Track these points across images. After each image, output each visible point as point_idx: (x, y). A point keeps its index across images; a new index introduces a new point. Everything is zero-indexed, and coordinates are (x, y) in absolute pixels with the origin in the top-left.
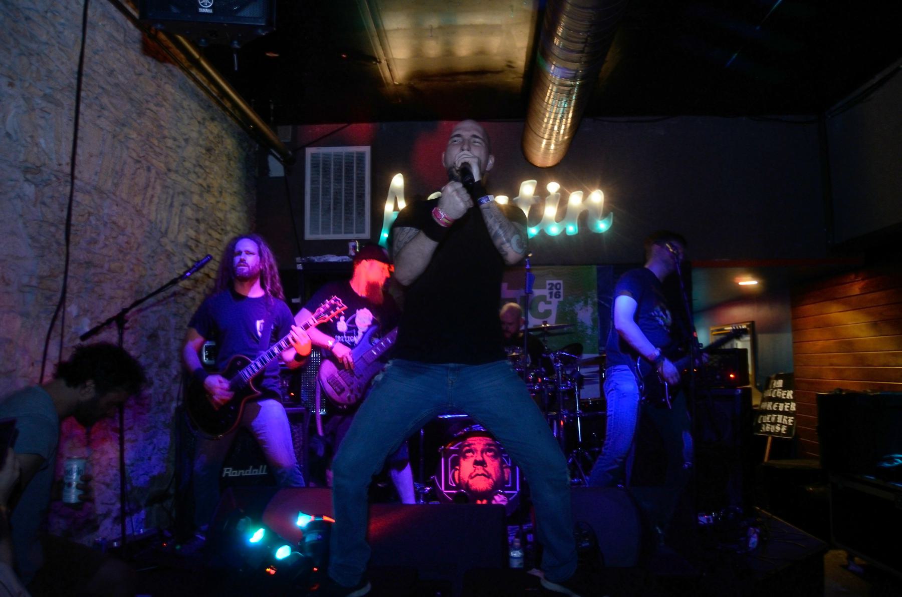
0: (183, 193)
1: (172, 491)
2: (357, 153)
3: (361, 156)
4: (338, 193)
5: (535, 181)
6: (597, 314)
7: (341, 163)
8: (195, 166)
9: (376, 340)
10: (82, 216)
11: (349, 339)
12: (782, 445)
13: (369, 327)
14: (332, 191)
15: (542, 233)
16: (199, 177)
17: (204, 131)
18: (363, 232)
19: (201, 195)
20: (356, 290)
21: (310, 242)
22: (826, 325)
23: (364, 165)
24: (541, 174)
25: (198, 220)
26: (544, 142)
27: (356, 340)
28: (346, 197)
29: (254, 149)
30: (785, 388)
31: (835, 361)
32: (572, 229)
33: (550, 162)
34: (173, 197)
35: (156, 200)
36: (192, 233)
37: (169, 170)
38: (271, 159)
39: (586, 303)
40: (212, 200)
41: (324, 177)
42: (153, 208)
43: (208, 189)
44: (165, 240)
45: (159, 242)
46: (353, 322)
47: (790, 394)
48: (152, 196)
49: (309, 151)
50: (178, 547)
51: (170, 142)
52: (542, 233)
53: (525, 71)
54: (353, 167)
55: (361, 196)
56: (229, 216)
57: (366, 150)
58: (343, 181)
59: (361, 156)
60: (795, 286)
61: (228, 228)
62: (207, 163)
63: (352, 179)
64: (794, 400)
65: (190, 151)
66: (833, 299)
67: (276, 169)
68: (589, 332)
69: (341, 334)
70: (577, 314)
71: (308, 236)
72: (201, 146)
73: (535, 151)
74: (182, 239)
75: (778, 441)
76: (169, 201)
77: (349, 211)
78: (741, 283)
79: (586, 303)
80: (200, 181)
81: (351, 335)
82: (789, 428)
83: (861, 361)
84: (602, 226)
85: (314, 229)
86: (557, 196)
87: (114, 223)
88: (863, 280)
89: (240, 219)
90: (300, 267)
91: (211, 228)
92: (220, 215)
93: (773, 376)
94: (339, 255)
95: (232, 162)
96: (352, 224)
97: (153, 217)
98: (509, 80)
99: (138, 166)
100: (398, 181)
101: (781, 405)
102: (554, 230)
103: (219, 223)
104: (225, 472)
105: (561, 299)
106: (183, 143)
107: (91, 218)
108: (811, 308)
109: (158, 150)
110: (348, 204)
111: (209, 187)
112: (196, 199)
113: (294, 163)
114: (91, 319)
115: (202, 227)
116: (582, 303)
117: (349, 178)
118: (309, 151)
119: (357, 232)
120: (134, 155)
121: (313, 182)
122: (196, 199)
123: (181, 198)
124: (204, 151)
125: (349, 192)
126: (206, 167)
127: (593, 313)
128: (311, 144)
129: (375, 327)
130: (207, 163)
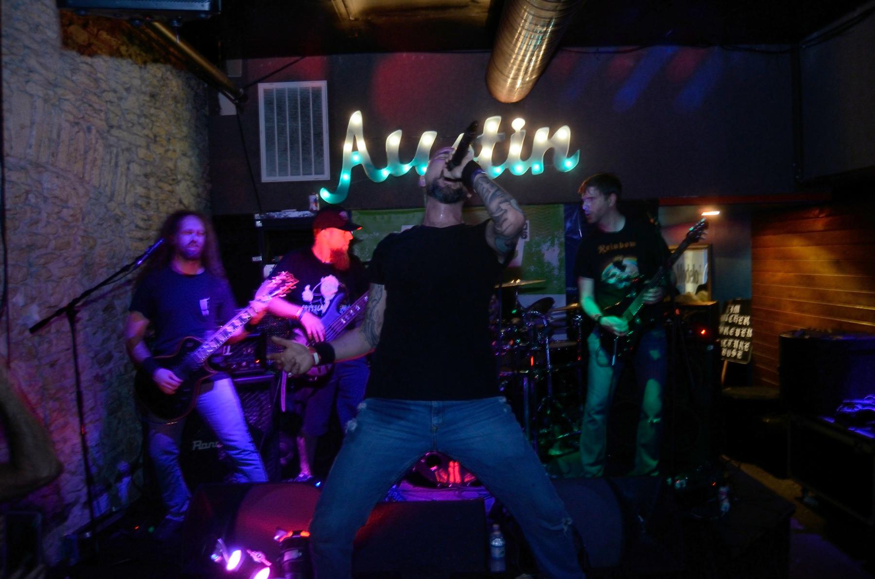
0: (128, 150)
1: (141, 461)
2: (313, 88)
3: (317, 93)
4: (294, 132)
5: (499, 118)
6: (564, 254)
7: (296, 100)
8: (139, 116)
9: (344, 308)
10: (20, 196)
11: (317, 309)
12: (740, 371)
13: (337, 294)
15: (507, 172)
16: (144, 128)
17: (146, 75)
18: (322, 173)
19: (148, 147)
20: (319, 257)
22: (786, 257)
23: (321, 102)
24: (507, 111)
25: (146, 176)
26: (509, 80)
27: (324, 308)
28: (303, 137)
29: (204, 91)
30: (742, 313)
31: (794, 293)
32: (538, 168)
33: (515, 98)
34: (117, 156)
35: (99, 162)
36: (140, 190)
37: (112, 127)
38: (221, 96)
39: (553, 244)
40: (161, 150)
41: (278, 115)
42: (96, 172)
43: (155, 139)
44: (112, 205)
46: (318, 291)
47: (747, 320)
48: (95, 160)
49: (262, 87)
50: (151, 529)
51: (110, 96)
52: (507, 172)
53: (491, 5)
55: (319, 135)
56: (179, 164)
57: (323, 85)
59: (317, 93)
60: (759, 215)
61: (179, 177)
62: (153, 111)
63: (309, 117)
64: (751, 326)
65: (131, 102)
66: (796, 232)
67: (228, 108)
68: (556, 272)
69: (307, 303)
70: (543, 255)
71: (265, 178)
72: (145, 93)
73: (499, 88)
74: (129, 199)
75: (734, 365)
76: (113, 161)
77: (306, 151)
78: (704, 214)
79: (553, 244)
80: (146, 132)
81: (318, 304)
82: (745, 354)
83: (822, 296)
84: (569, 164)
85: (271, 171)
86: (522, 133)
87: (56, 197)
88: (826, 216)
89: (191, 164)
90: (259, 224)
91: (160, 180)
92: (170, 164)
93: (731, 301)
94: (299, 210)
95: (179, 105)
96: (311, 165)
97: (95, 182)
98: (473, 15)
99: (76, 129)
100: (356, 119)
101: (738, 331)
102: (519, 169)
103: (169, 173)
104: (195, 446)
105: (528, 239)
106: (125, 94)
107: (30, 196)
108: (770, 239)
109: (97, 107)
110: (306, 143)
111: (155, 136)
112: (142, 152)
113: (245, 100)
114: (39, 305)
115: (152, 181)
116: (549, 243)
117: (305, 116)
118: (262, 87)
119: (316, 173)
120: (71, 118)
122: (142, 152)
123: (127, 154)
124: (147, 98)
125: (306, 132)
126: (152, 115)
127: (560, 254)
128: (263, 80)
129: (341, 295)
130: (153, 111)
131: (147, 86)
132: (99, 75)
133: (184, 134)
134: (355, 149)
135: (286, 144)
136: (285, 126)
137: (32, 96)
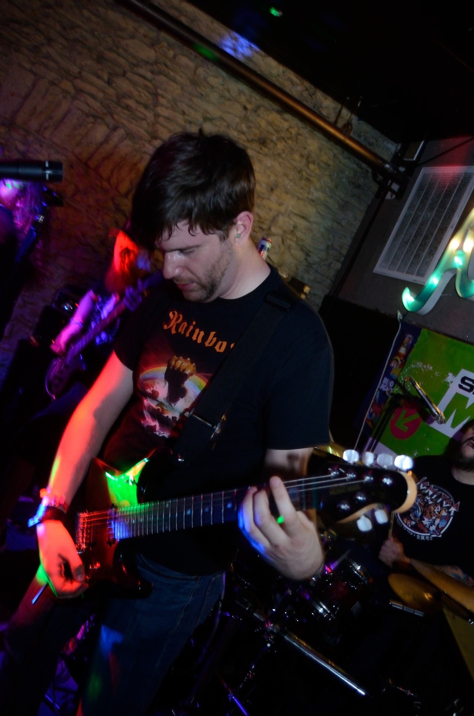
7: (444, 187)
14: (420, 220)
21: (377, 275)
45: (113, 199)
49: (424, 171)
54: (453, 192)
55: (443, 230)
56: (281, 219)
58: (436, 209)
63: (445, 208)
71: (379, 268)
77: (423, 246)
95: (312, 166)
96: (418, 264)
109: (138, 114)
110: (426, 238)
117: (443, 205)
120: (86, 109)
121: (410, 208)
131: (249, 128)
132: (159, 91)
133: (310, 196)
134: (460, 248)
135: (411, 236)
136: (421, 215)
137: (35, 74)
